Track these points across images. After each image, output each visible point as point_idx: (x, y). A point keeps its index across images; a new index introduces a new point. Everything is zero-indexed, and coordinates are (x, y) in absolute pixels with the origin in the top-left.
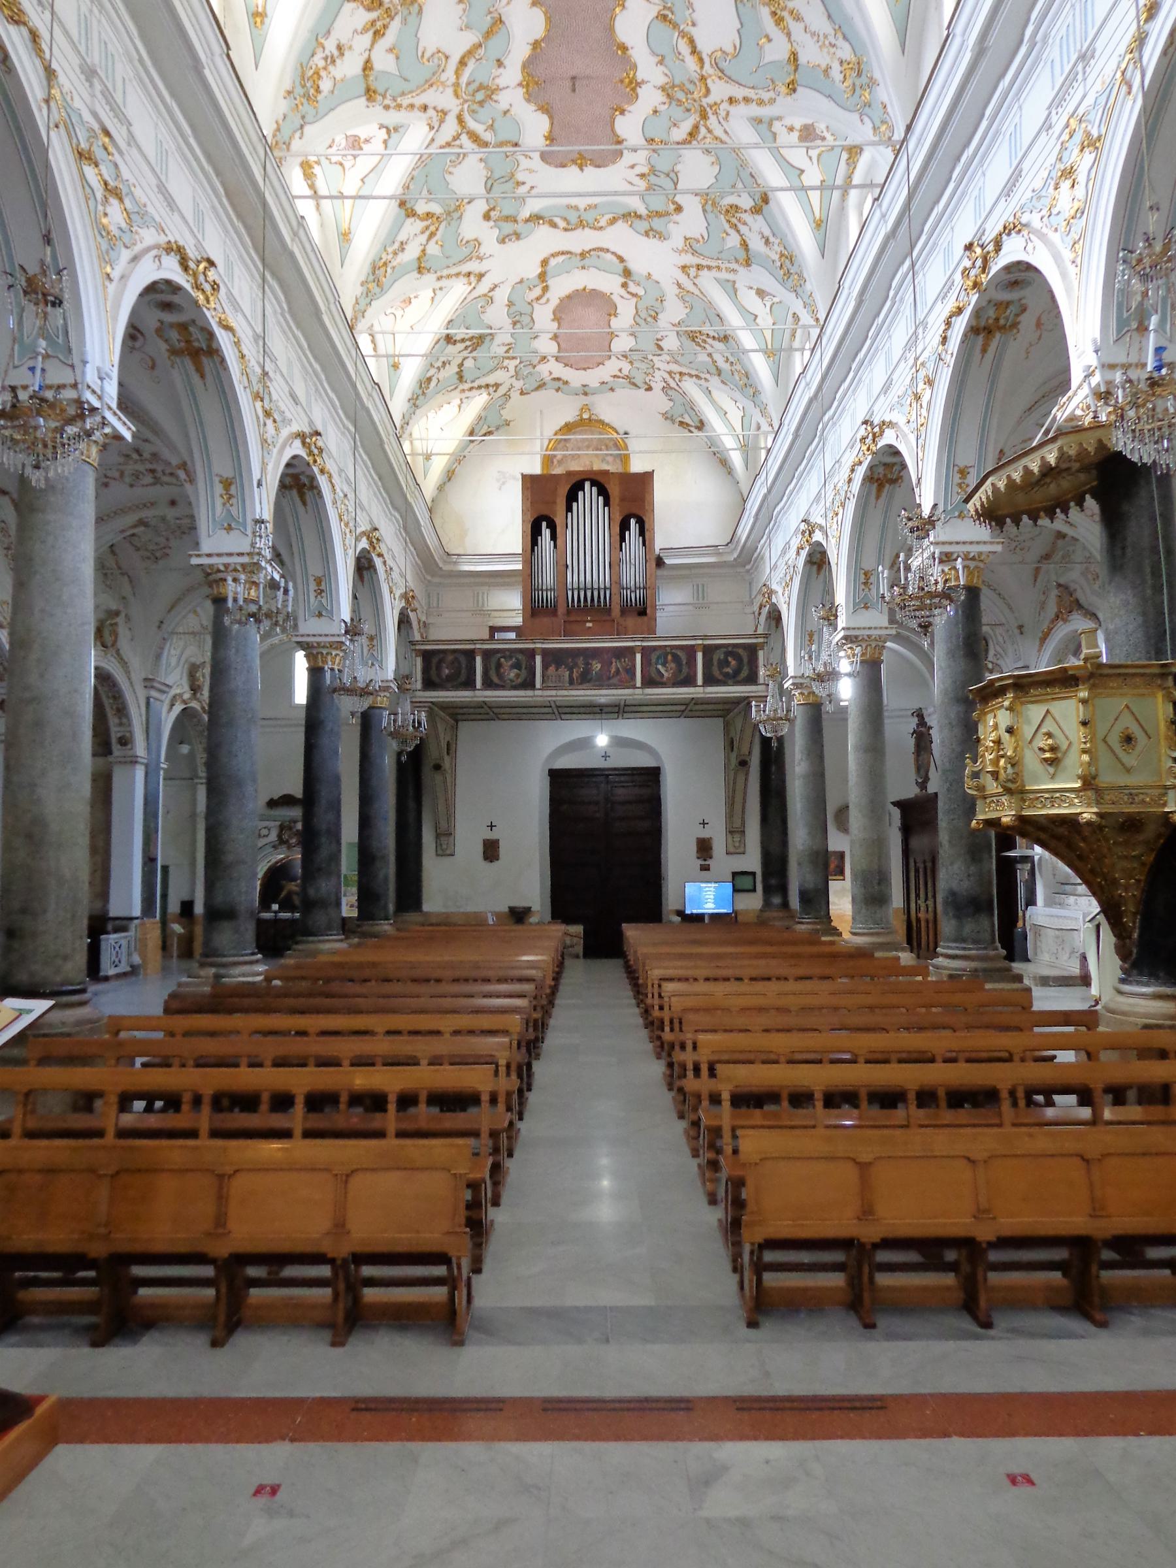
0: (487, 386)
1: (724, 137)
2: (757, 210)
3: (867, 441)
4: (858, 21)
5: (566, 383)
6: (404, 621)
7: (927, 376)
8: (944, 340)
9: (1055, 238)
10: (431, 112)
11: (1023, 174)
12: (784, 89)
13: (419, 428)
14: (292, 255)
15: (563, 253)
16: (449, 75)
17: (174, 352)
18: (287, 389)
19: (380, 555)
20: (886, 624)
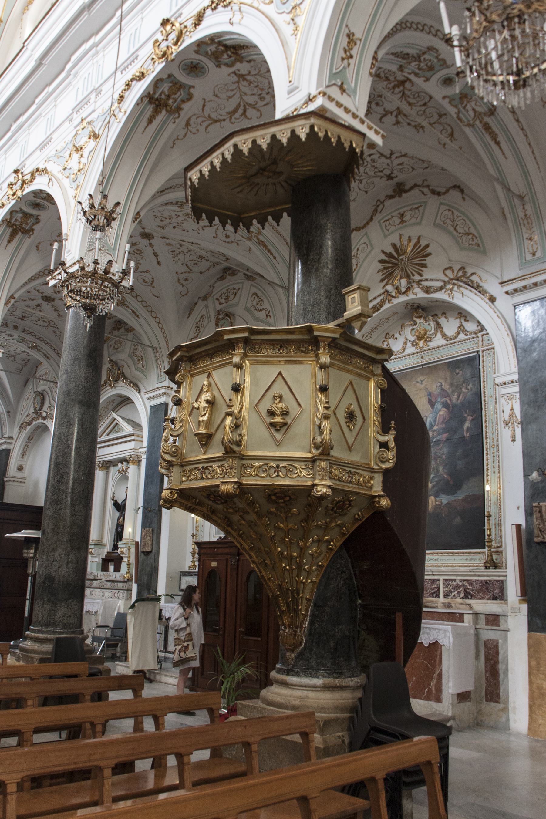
3: (14, 187)
7: (93, 131)
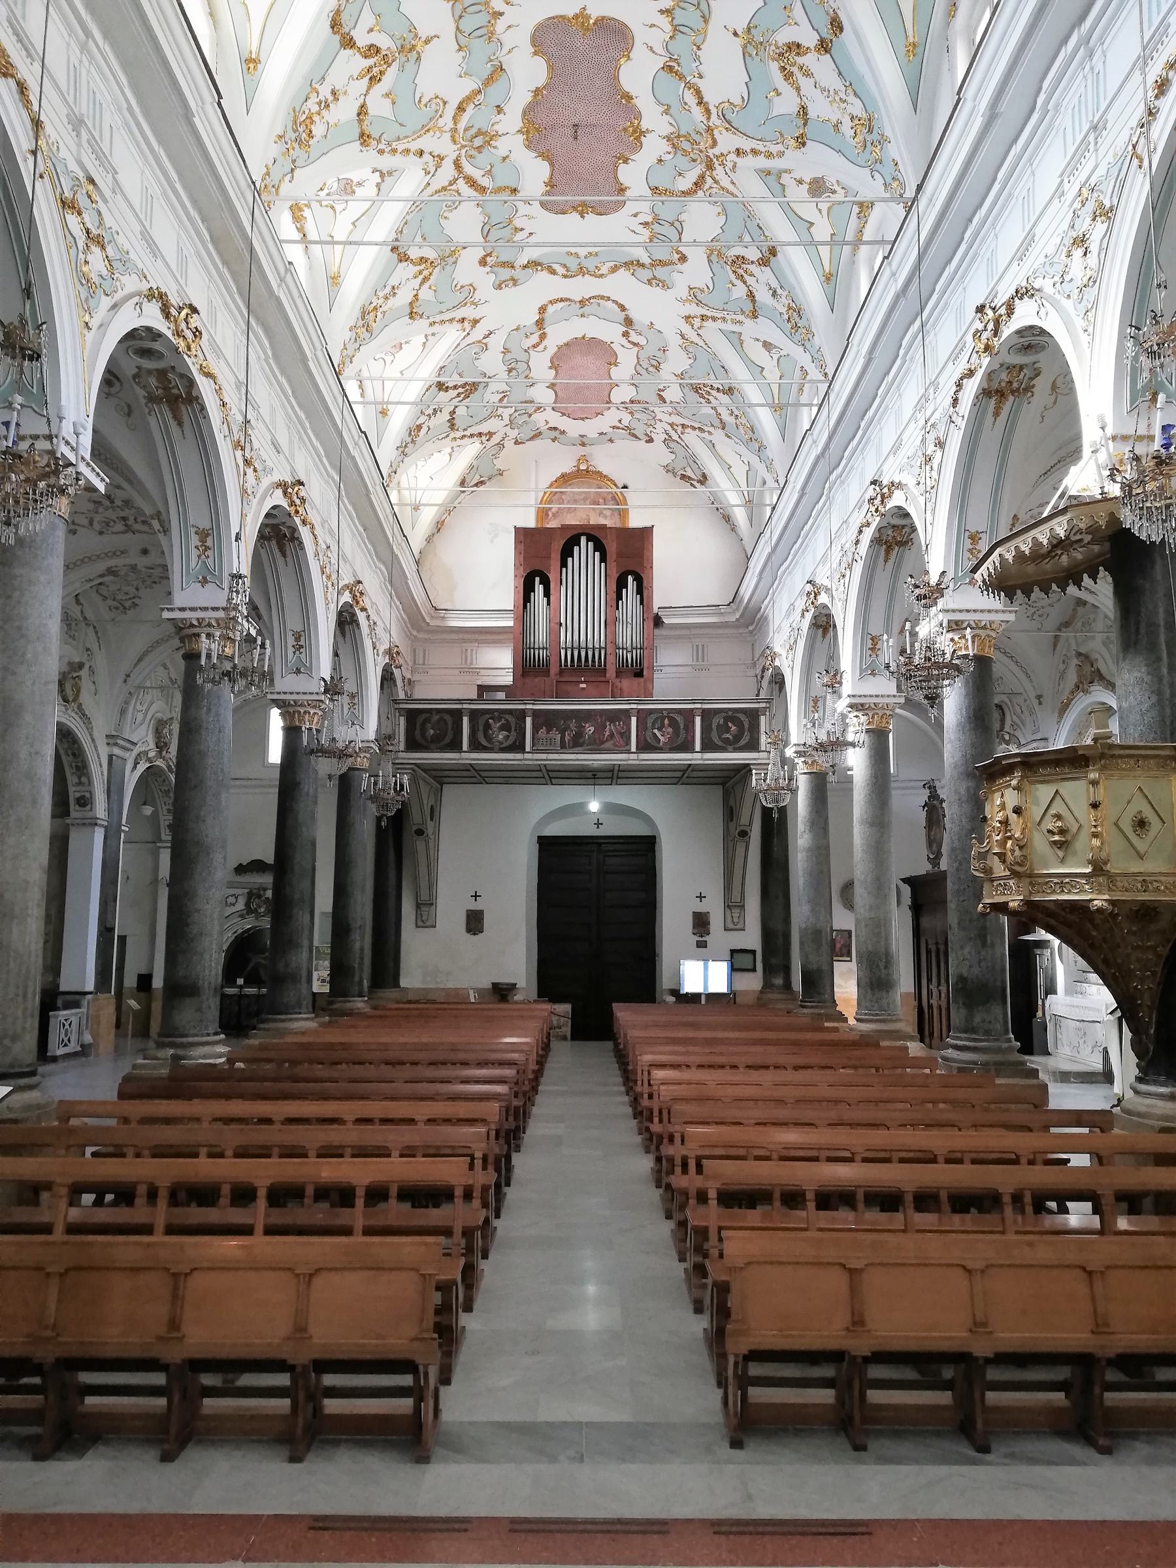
0: (480, 434)
1: (731, 188)
2: (764, 262)
4: (868, 79)
5: (563, 432)
6: (387, 678)
7: (938, 438)
8: (955, 402)
9: (1068, 305)
10: (427, 157)
11: (1036, 239)
12: (792, 143)
13: (405, 478)
14: (278, 300)
15: (562, 300)
16: (447, 121)
17: (152, 399)
18: (269, 438)
19: (363, 609)
20: (894, 691)
